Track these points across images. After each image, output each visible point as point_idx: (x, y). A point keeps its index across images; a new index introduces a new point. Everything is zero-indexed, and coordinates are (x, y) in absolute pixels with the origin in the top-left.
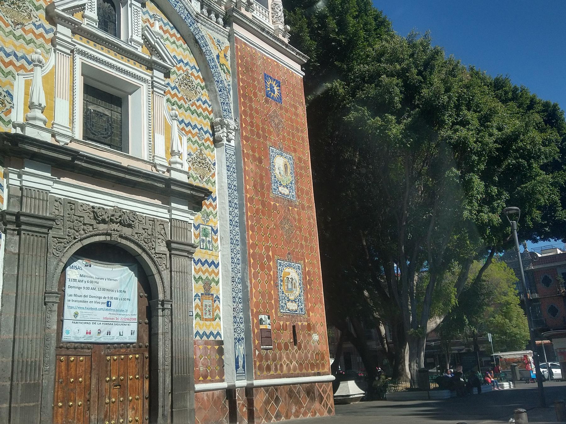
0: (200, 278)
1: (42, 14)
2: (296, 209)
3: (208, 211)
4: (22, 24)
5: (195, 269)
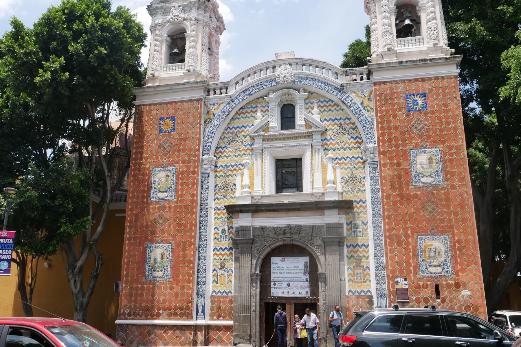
1: (248, 138)
2: (442, 191)
5: (348, 251)
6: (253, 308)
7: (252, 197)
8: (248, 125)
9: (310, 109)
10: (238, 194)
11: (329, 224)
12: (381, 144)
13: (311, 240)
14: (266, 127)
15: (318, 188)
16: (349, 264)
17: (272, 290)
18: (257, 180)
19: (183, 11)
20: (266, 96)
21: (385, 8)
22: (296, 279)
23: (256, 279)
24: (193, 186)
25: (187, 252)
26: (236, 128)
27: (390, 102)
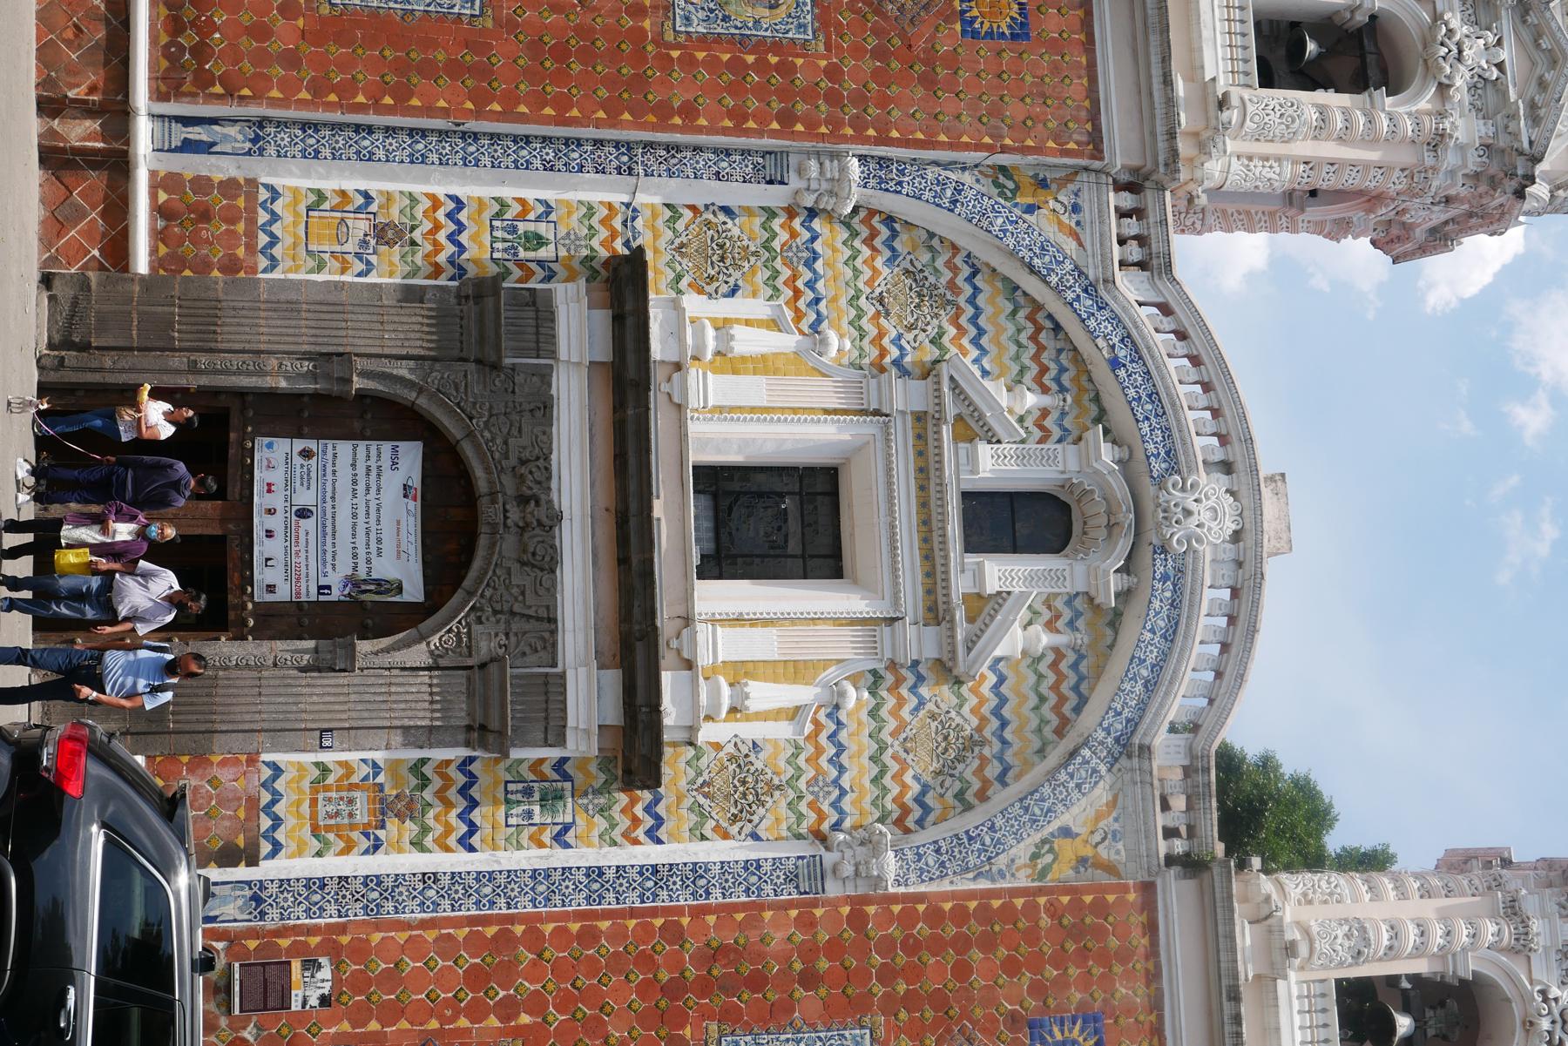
0: (424, 782)
1: (931, 353)
3: (616, 812)
4: (888, 314)
5: (448, 763)
6: (203, 360)
7: (678, 367)
8: (984, 351)
9: (1047, 615)
10: (693, 304)
11: (564, 686)
12: (896, 909)
13: (495, 612)
14: (974, 428)
15: (717, 645)
16: (394, 765)
17: (282, 445)
18: (753, 389)
19: (1480, 83)
20: (1106, 432)
21: (1463, 935)
22: (329, 547)
23: (328, 377)
24: (731, 114)
25: (445, 81)
26: (972, 301)
27: (1071, 947)
